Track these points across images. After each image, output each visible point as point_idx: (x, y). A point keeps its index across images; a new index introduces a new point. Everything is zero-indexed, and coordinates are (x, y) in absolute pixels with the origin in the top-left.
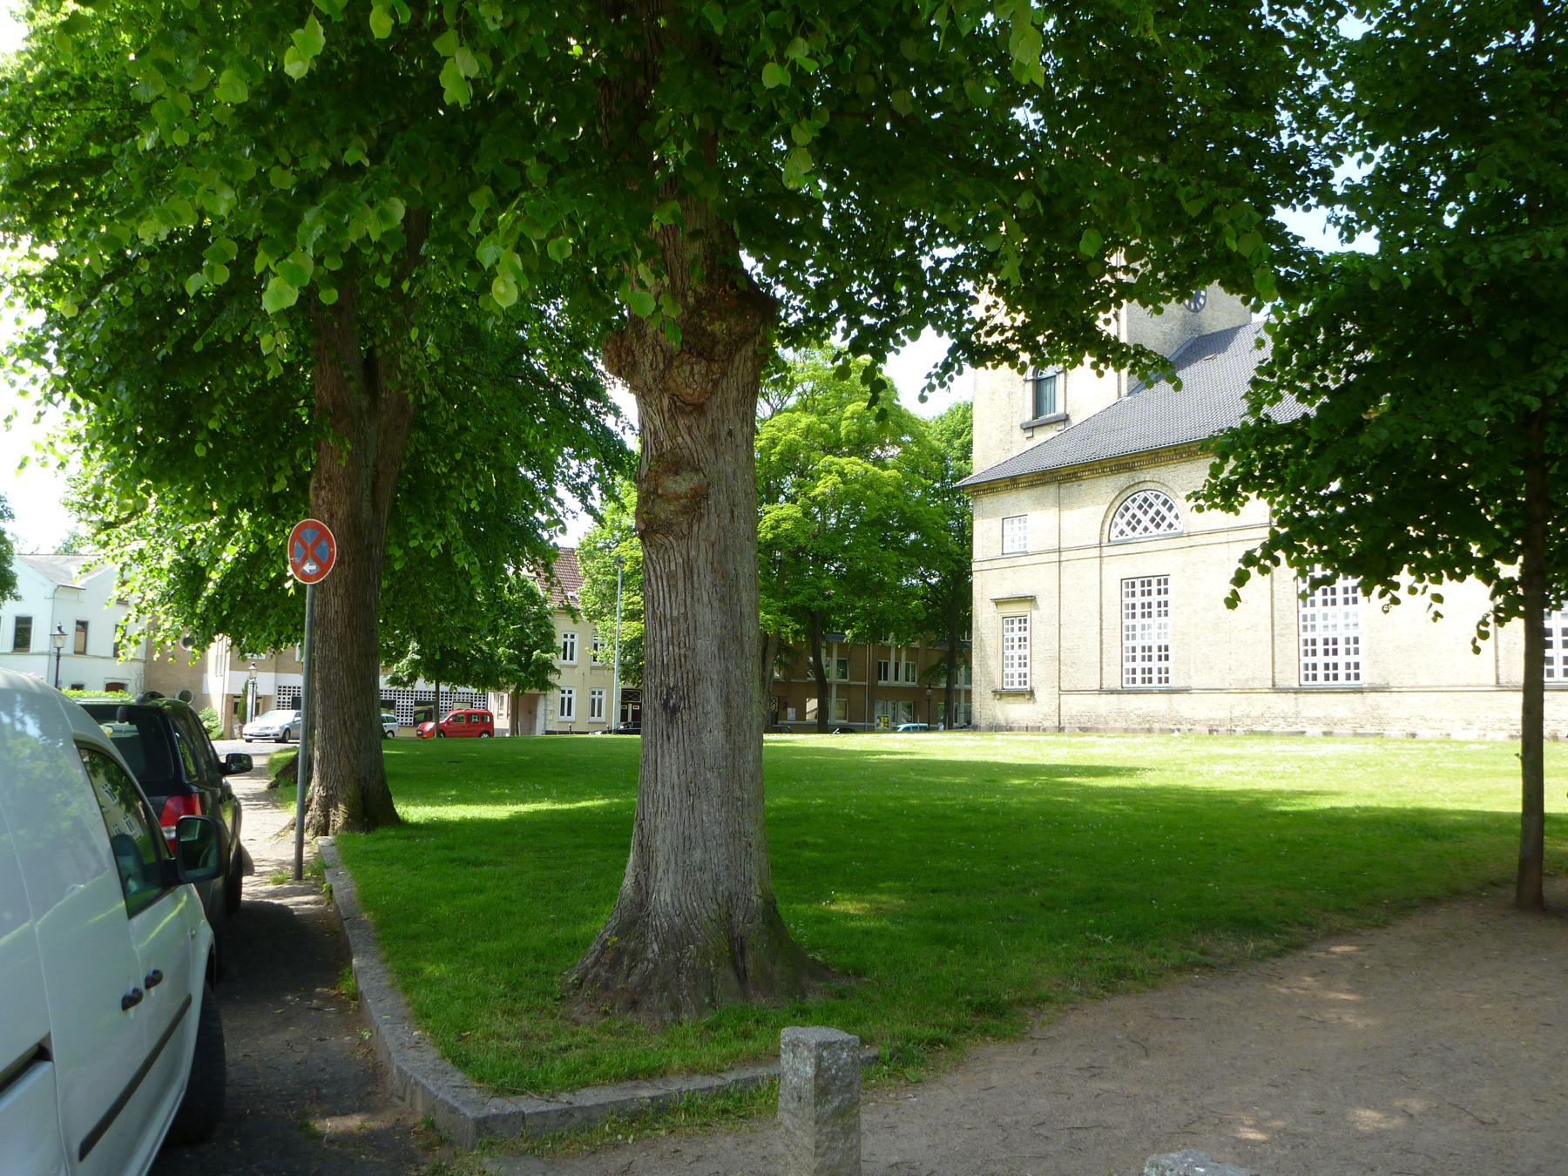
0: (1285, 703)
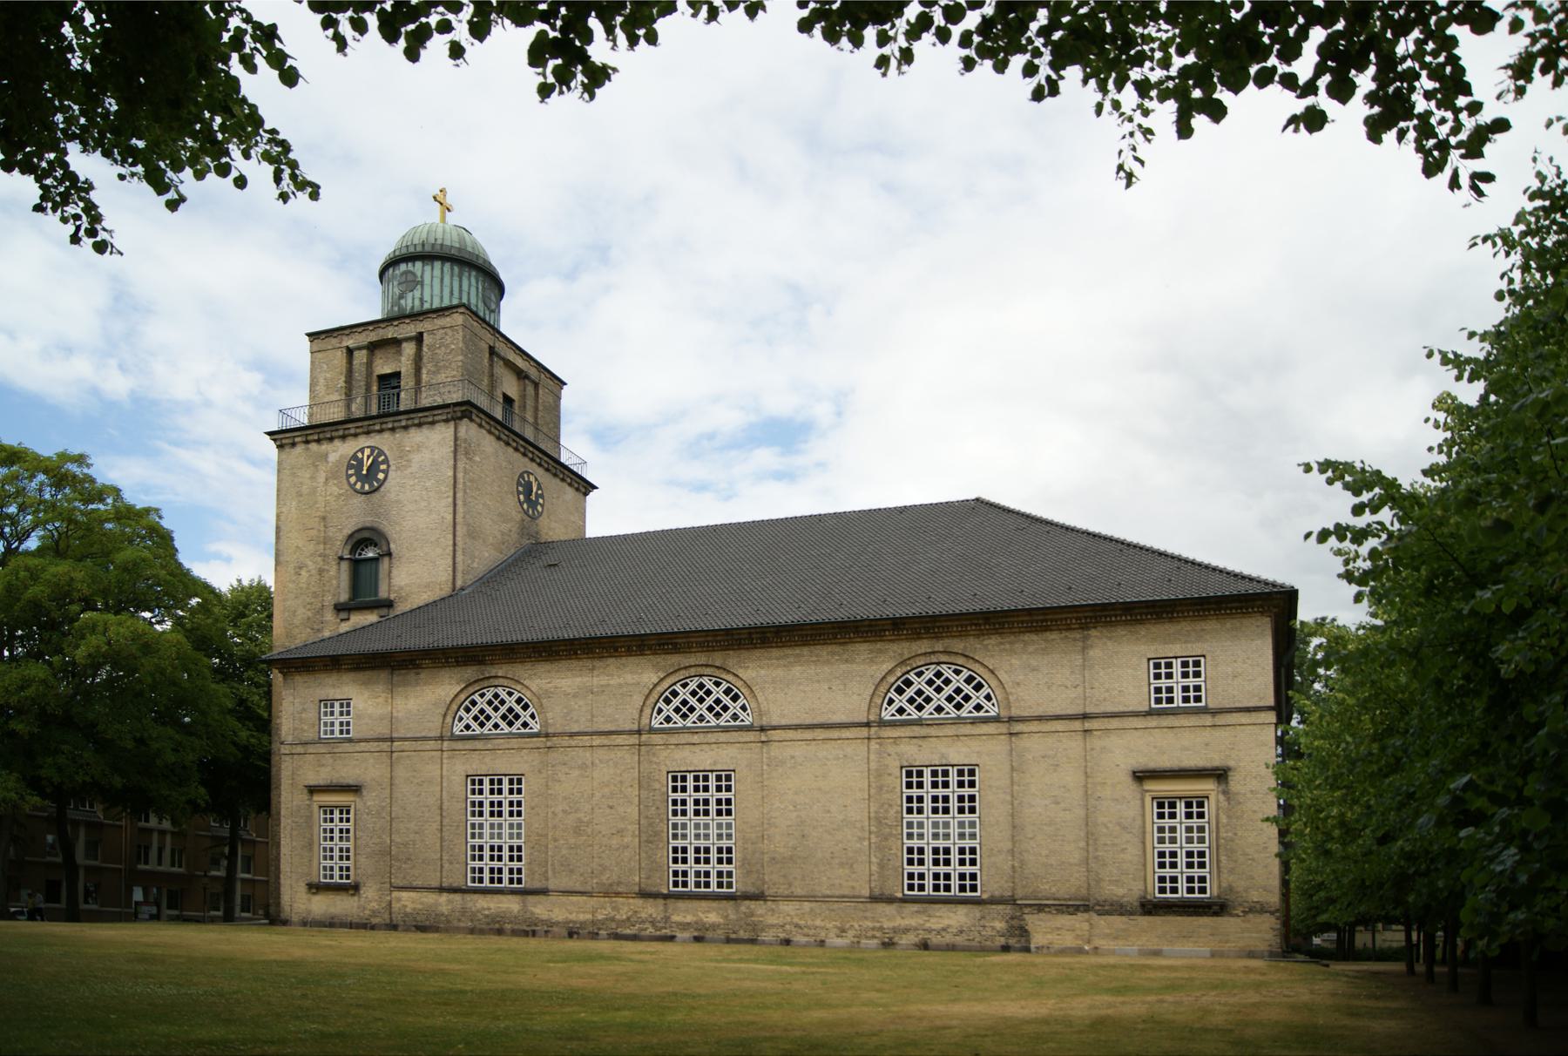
0: (651, 909)
